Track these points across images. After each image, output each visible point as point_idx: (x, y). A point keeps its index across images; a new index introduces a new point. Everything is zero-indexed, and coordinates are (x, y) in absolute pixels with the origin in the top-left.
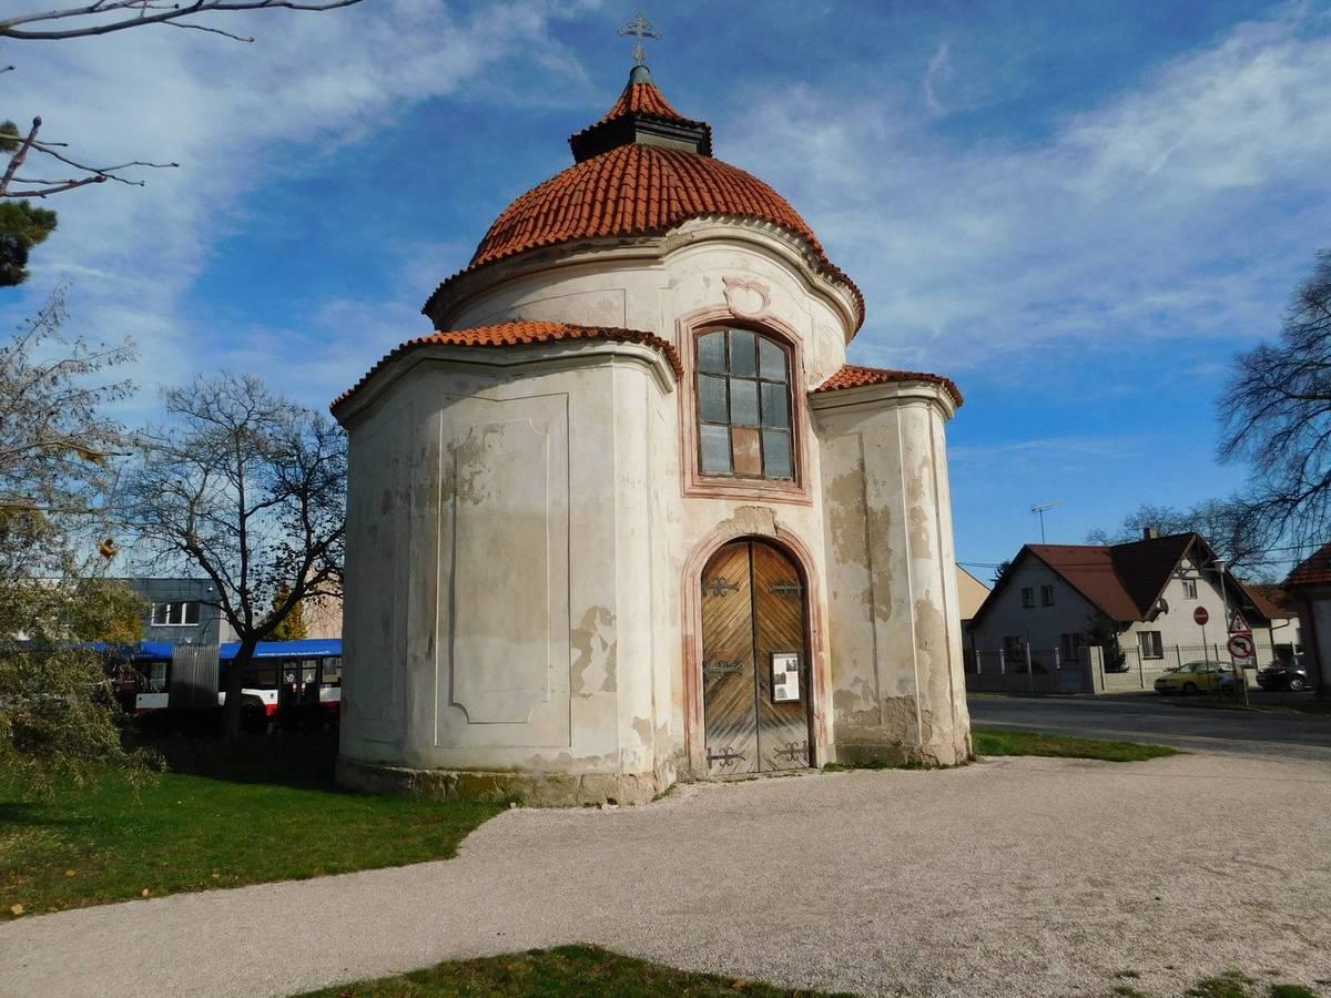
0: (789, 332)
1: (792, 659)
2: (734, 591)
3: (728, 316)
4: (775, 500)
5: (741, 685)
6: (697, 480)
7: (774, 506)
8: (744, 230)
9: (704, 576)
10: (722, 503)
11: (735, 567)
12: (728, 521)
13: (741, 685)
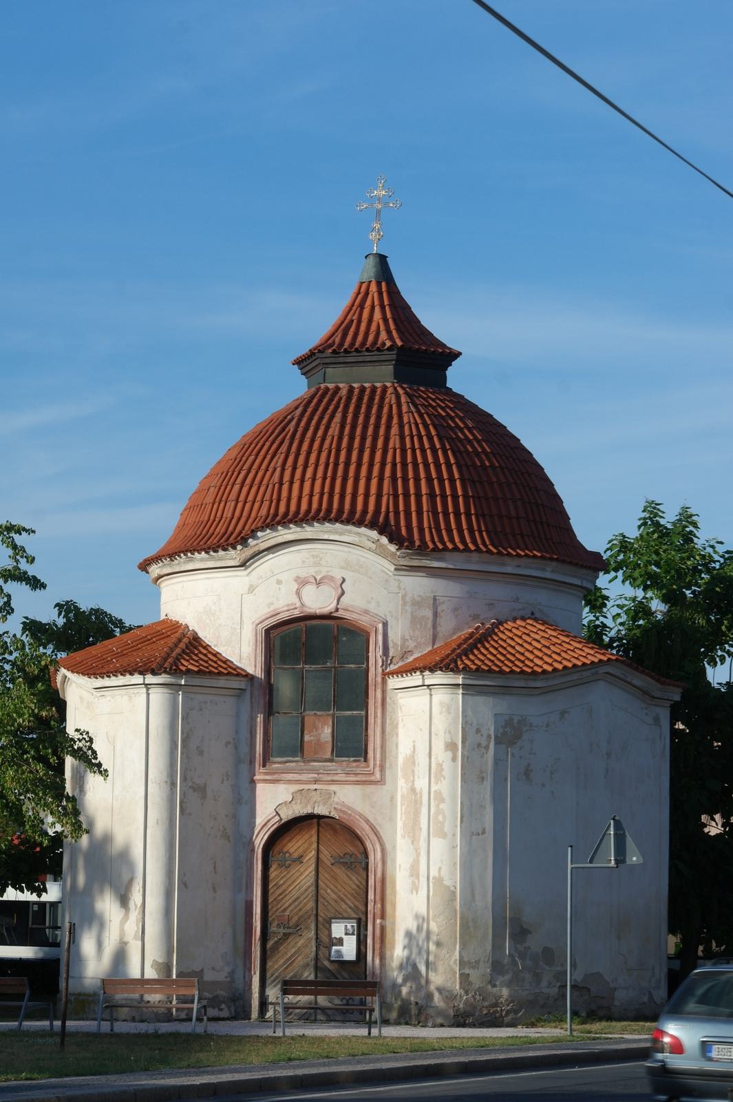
1: (351, 925)
3: (296, 613)
4: (333, 782)
5: (299, 944)
7: (333, 788)
11: (300, 843)
12: (285, 803)
13: (299, 944)
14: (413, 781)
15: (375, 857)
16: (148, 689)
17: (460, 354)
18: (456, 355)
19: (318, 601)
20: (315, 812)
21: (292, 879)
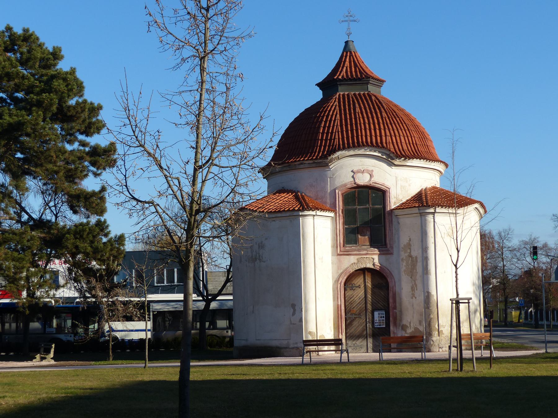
0: (383, 187)
2: (358, 288)
6: (342, 249)
8: (361, 152)
9: (345, 284)
10: (352, 257)
14: (410, 252)
15: (391, 285)
16: (314, 217)
17: (316, 85)
18: (318, 85)
19: (363, 180)
20: (367, 267)
21: (356, 295)
